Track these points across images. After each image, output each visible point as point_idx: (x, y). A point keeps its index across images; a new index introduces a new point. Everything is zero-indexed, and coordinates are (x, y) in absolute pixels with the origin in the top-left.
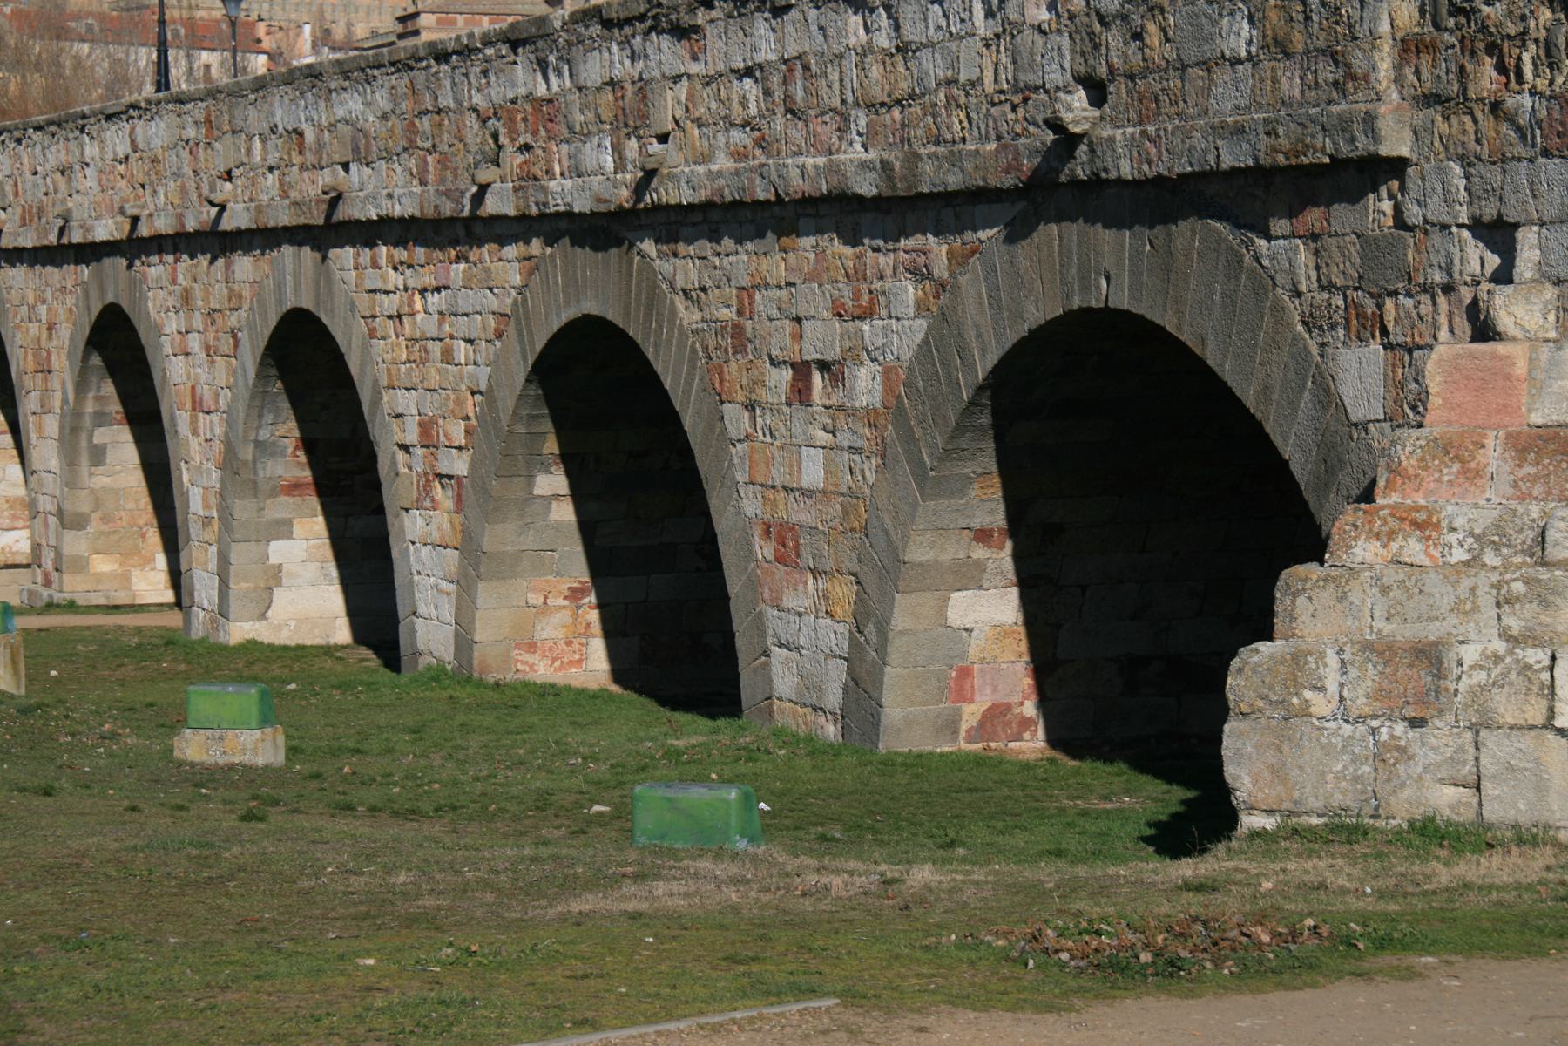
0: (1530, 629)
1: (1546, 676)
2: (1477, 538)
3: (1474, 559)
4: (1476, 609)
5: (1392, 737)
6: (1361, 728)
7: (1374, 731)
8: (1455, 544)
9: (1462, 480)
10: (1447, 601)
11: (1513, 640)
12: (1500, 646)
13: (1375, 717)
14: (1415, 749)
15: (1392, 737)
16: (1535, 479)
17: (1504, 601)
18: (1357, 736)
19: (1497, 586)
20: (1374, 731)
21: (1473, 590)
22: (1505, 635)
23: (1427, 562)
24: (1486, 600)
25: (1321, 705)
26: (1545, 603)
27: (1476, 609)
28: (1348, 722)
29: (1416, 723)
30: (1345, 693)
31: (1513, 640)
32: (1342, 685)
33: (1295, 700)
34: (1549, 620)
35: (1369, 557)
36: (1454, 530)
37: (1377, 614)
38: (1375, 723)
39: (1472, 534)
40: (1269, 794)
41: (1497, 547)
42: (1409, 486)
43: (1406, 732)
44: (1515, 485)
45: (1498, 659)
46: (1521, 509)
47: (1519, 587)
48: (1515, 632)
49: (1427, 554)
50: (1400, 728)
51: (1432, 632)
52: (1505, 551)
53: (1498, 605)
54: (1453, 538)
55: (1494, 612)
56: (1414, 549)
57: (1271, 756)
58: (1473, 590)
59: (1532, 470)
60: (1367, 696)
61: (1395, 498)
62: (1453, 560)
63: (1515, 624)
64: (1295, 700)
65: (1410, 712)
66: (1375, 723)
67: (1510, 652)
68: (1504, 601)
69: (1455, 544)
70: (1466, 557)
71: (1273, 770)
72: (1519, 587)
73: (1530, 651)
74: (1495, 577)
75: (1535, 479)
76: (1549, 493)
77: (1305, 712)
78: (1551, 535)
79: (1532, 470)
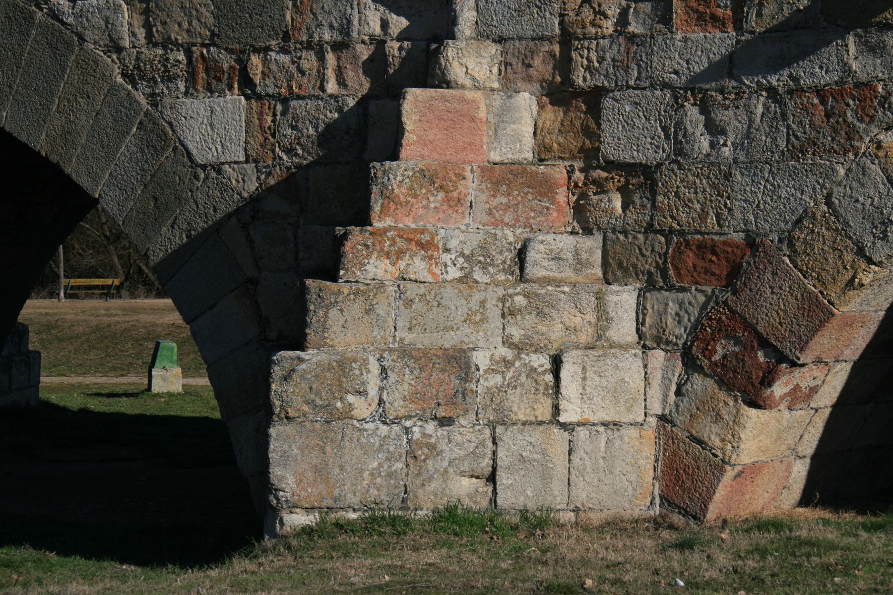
0: (529, 338)
1: (549, 378)
2: (467, 258)
3: (466, 276)
4: (484, 320)
5: (424, 435)
6: (396, 428)
7: (407, 431)
8: (449, 263)
9: (445, 207)
10: (463, 311)
11: (518, 348)
12: (509, 354)
13: (409, 417)
14: (443, 446)
15: (424, 435)
16: (508, 207)
17: (509, 313)
18: (393, 435)
19: (503, 300)
20: (407, 431)
21: (483, 303)
22: (507, 342)
23: (430, 279)
24: (493, 311)
25: (362, 407)
26: (540, 314)
27: (484, 320)
28: (385, 423)
29: (445, 422)
30: (385, 397)
31: (518, 348)
32: (381, 389)
33: (339, 404)
34: (545, 329)
35: (380, 273)
36: (447, 250)
37: (400, 325)
38: (408, 423)
39: (462, 255)
40: (313, 492)
41: (484, 267)
42: (401, 211)
43: (436, 431)
44: (490, 213)
45: (508, 364)
46: (499, 234)
47: (520, 300)
48: (516, 340)
49: (430, 271)
50: (431, 427)
51: (449, 340)
52: (491, 269)
53: (503, 316)
54: (446, 258)
55: (499, 323)
56: (418, 267)
57: (314, 457)
58: (483, 303)
59: (504, 200)
60: (404, 399)
61: (389, 222)
62: (449, 277)
63: (516, 333)
64: (339, 404)
65: (441, 413)
66: (408, 423)
67: (518, 357)
68: (509, 313)
69: (449, 263)
70: (459, 274)
71: (316, 469)
72: (520, 300)
73: (534, 357)
74: (500, 292)
75: (508, 207)
76: (517, 220)
77: (347, 414)
78: (532, 255)
79: (504, 200)
